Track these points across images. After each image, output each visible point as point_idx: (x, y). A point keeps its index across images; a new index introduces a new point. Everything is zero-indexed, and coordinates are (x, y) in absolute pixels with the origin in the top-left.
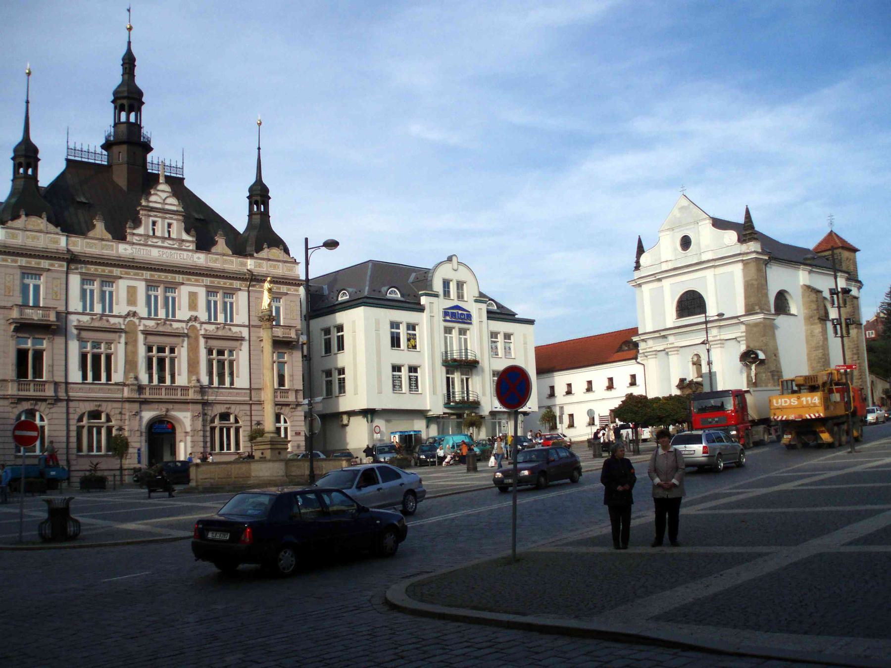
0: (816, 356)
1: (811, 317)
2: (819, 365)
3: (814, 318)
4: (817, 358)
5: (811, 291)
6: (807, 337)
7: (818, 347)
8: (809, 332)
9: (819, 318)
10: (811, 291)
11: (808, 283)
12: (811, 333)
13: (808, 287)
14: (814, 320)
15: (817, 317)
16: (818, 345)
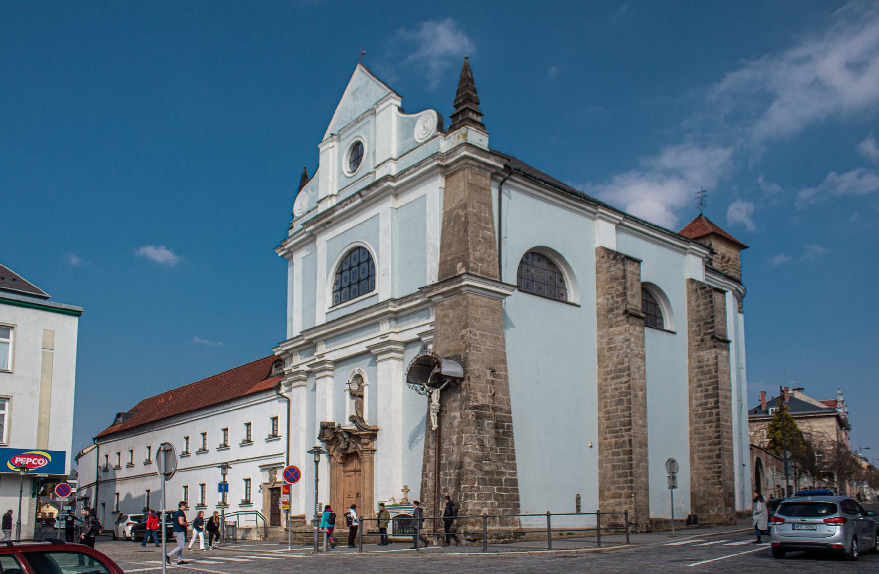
0: (616, 389)
1: (611, 310)
2: (620, 407)
3: (616, 312)
4: (617, 393)
5: (615, 258)
6: (600, 350)
7: (621, 370)
8: (605, 340)
9: (626, 312)
10: (615, 258)
11: (613, 246)
12: (608, 344)
13: (608, 251)
14: (617, 316)
15: (621, 312)
16: (619, 367)
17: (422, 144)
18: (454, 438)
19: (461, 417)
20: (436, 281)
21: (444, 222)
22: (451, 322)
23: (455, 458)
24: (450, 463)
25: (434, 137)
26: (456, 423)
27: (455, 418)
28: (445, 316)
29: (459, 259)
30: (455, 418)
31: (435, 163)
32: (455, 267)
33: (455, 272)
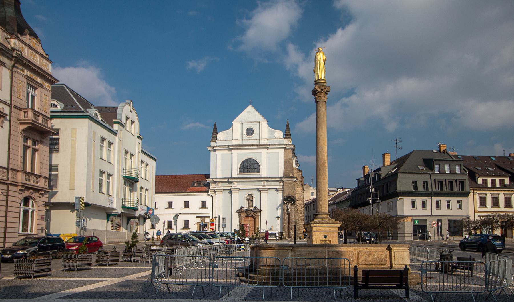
17: (278, 139)
18: (293, 215)
19: (295, 210)
20: (283, 176)
21: (284, 161)
22: (289, 187)
23: (294, 220)
24: (292, 221)
25: (281, 139)
26: (293, 212)
27: (293, 211)
28: (287, 185)
29: (291, 172)
30: (293, 211)
31: (285, 147)
32: (290, 174)
33: (290, 175)
